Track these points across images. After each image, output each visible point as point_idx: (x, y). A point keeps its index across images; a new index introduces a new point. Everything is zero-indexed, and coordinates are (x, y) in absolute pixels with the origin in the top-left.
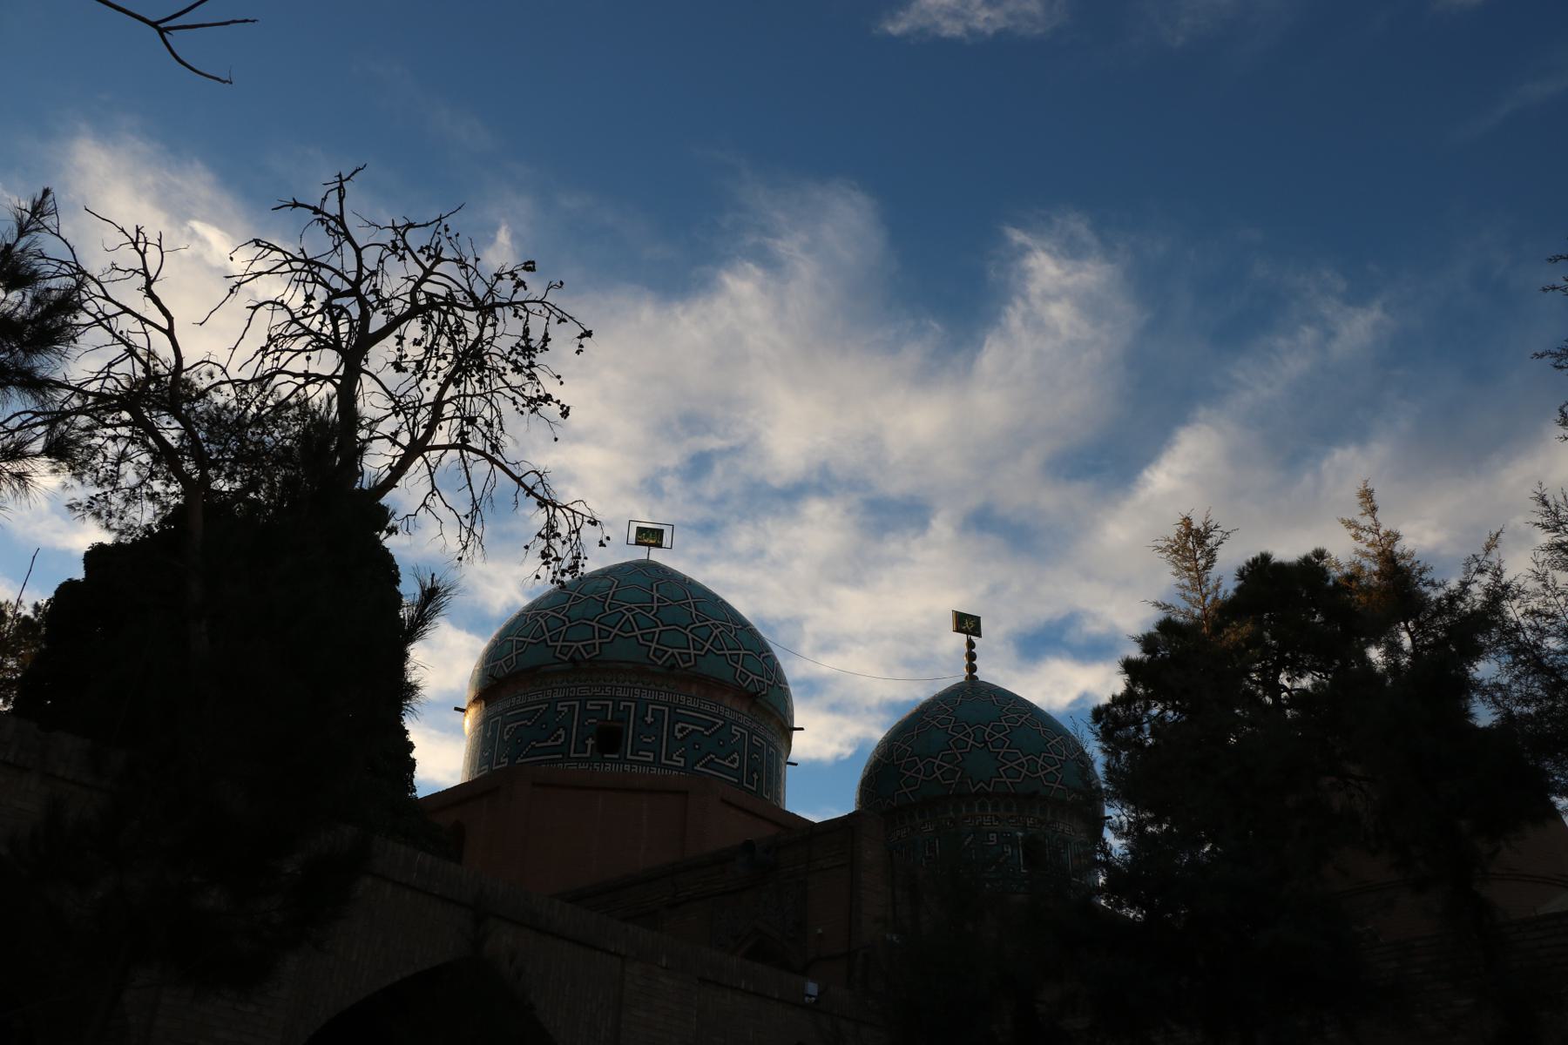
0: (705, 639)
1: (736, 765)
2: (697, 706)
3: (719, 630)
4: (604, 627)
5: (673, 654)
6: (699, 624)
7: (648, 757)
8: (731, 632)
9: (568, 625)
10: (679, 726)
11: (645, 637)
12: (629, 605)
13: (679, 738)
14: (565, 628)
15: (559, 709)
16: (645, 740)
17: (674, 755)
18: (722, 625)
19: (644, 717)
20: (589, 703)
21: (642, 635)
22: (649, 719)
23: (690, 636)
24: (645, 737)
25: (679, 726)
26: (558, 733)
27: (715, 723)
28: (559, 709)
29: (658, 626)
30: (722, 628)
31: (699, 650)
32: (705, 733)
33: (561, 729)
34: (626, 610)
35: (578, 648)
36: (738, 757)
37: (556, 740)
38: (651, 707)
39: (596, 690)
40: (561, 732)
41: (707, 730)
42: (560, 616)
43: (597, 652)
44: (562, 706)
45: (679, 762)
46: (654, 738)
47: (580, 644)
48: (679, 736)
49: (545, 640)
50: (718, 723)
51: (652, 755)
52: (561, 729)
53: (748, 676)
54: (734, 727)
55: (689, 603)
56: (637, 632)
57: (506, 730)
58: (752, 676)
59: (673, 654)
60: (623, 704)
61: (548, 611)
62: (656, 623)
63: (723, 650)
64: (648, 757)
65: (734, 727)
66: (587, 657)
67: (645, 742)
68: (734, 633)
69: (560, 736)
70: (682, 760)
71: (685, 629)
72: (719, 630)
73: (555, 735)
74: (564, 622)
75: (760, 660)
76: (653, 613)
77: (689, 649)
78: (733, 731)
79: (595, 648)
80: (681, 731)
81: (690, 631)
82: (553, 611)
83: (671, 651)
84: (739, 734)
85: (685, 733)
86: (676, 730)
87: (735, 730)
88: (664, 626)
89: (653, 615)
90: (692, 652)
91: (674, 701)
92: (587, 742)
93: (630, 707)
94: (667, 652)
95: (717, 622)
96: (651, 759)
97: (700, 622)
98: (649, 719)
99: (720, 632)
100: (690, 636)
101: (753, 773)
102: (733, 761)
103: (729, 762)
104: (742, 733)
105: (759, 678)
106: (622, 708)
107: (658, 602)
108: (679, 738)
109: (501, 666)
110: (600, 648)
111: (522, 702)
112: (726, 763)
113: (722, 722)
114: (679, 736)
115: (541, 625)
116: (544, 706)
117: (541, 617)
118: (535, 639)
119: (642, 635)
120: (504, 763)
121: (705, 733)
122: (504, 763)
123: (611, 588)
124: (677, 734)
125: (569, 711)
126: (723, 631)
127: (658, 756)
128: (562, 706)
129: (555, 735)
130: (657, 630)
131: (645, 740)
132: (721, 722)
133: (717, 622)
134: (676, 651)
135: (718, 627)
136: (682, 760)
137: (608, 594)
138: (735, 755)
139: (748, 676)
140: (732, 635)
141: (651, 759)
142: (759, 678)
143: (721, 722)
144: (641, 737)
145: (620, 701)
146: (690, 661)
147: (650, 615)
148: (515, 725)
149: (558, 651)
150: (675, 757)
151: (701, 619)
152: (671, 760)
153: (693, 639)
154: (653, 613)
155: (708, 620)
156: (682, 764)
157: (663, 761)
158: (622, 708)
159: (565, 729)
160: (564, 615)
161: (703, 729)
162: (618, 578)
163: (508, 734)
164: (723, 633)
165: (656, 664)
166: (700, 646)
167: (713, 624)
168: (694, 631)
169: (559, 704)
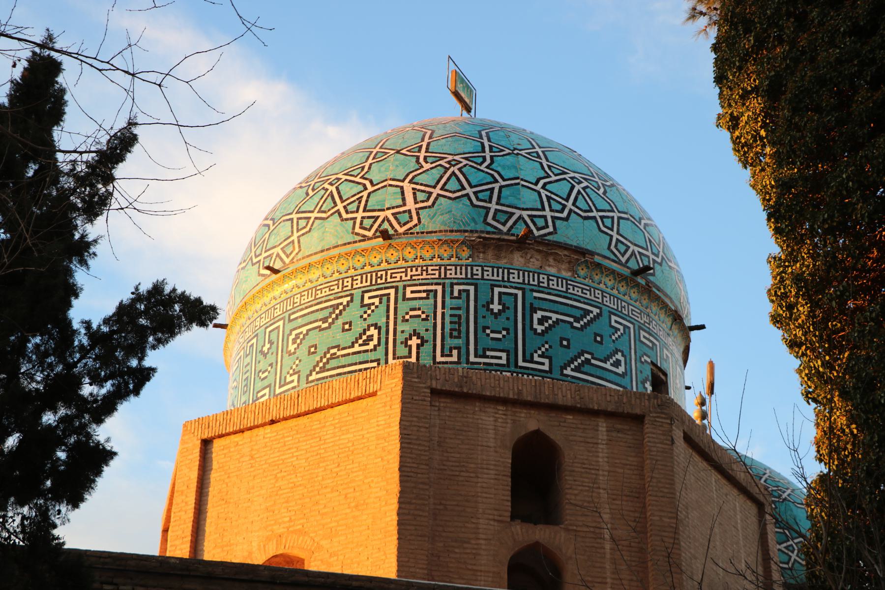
0: (565, 197)
1: (621, 370)
2: (564, 289)
3: (583, 185)
4: (418, 187)
5: (520, 218)
6: (554, 178)
7: (500, 358)
8: (599, 189)
9: (370, 188)
10: (539, 314)
11: (480, 195)
12: (450, 158)
13: (539, 331)
14: (365, 194)
15: (366, 301)
16: (492, 335)
17: (536, 355)
18: (586, 179)
19: (488, 304)
20: (409, 290)
21: (475, 193)
22: (496, 307)
23: (542, 191)
24: (492, 332)
25: (539, 314)
26: (368, 333)
27: (588, 312)
28: (366, 301)
29: (496, 181)
30: (585, 184)
31: (557, 211)
32: (575, 324)
33: (372, 328)
34: (449, 162)
35: (386, 219)
36: (622, 359)
37: (365, 343)
38: (497, 290)
39: (414, 273)
40: (373, 331)
41: (577, 320)
42: (358, 179)
43: (415, 221)
44: (370, 298)
45: (543, 364)
46: (504, 333)
47: (389, 213)
48: (540, 329)
49: (338, 212)
50: (592, 312)
51: (504, 355)
52: (372, 328)
53: (628, 247)
54: (613, 318)
55: (537, 152)
56: (469, 190)
57: (293, 336)
58: (632, 247)
59: (520, 218)
60: (457, 288)
61: (340, 176)
62: (492, 176)
63: (591, 211)
64: (500, 358)
65: (613, 318)
66: (401, 230)
67: (493, 339)
68: (602, 190)
69: (370, 338)
70: (546, 361)
71: (536, 184)
72: (583, 185)
73: (364, 337)
74: (364, 185)
75: (642, 227)
76: (486, 164)
77: (543, 209)
78: (613, 324)
79: (411, 217)
80: (541, 322)
81: (543, 187)
82: (345, 174)
83: (518, 213)
84: (621, 328)
85: (546, 325)
86: (535, 321)
87: (616, 322)
88: (504, 180)
89: (487, 167)
90: (548, 213)
91: (531, 282)
92: (409, 342)
93: (468, 291)
94: (513, 214)
95: (577, 175)
96: (504, 361)
97: (556, 175)
98: (496, 307)
99: (584, 189)
100: (544, 193)
101: (643, 382)
102: (617, 364)
103: (612, 365)
104: (625, 327)
105: (641, 250)
106: (456, 294)
107: (491, 151)
108: (539, 331)
109: (278, 255)
110: (418, 214)
111: (310, 299)
112: (608, 366)
113: (598, 311)
114: (540, 329)
115: (331, 194)
116: (345, 301)
117: (331, 184)
118: (324, 212)
119: (475, 193)
120: (292, 381)
121: (575, 324)
122: (292, 381)
123: (423, 140)
124: (536, 326)
125: (380, 303)
126: (587, 187)
127: (512, 354)
128: (370, 298)
129: (364, 337)
130: (496, 186)
131: (492, 335)
132: (596, 311)
133: (577, 175)
134: (525, 214)
135: (580, 183)
136: (546, 361)
137: (421, 147)
138: (619, 356)
139: (628, 247)
140: (601, 191)
141: (504, 361)
142: (641, 250)
143: (596, 311)
144: (488, 331)
145: (452, 285)
146: (547, 226)
147: (482, 167)
148: (304, 330)
149: (358, 225)
150: (536, 358)
151: (557, 172)
152: (532, 361)
153: (549, 198)
154: (486, 164)
155: (564, 173)
156: (546, 368)
157: (521, 363)
158: (456, 294)
159: (376, 326)
160: (362, 177)
161: (572, 320)
162: (430, 128)
163: (294, 342)
164: (588, 190)
165: (500, 232)
166: (559, 207)
167: (572, 178)
168: (548, 187)
169: (367, 295)
